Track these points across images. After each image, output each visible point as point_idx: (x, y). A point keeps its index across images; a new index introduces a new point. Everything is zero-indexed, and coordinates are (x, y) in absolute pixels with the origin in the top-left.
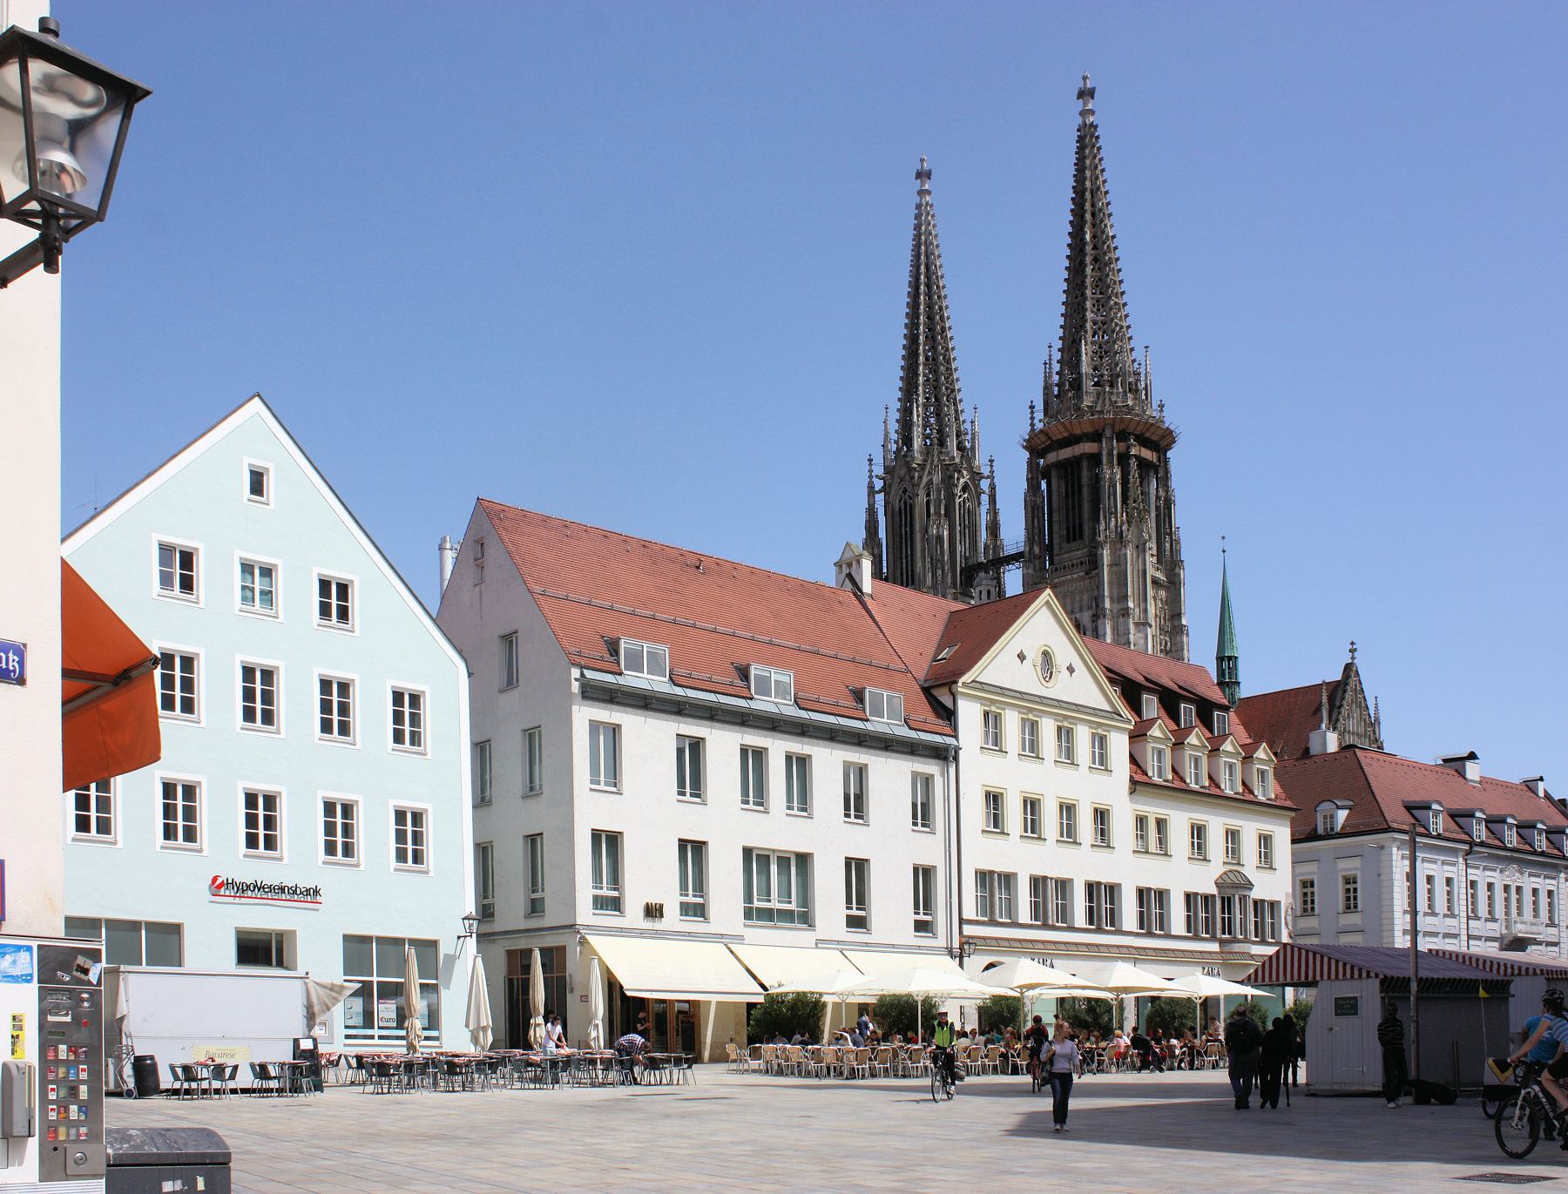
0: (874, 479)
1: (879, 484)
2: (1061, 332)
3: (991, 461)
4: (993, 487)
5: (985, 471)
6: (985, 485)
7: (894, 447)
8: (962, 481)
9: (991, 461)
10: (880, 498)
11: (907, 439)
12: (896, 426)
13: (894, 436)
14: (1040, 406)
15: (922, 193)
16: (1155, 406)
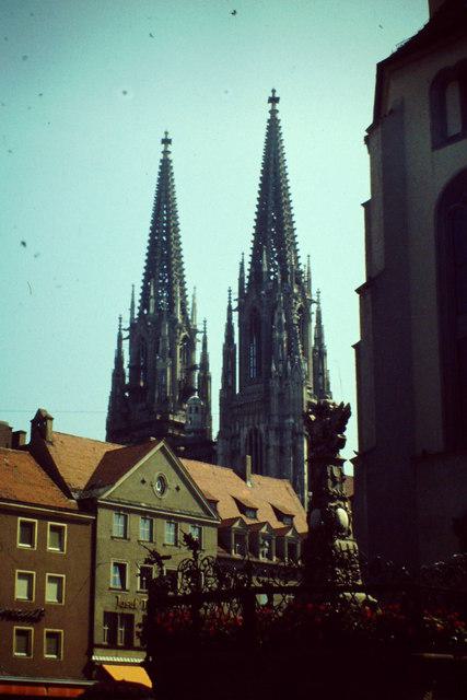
0: (123, 332)
1: (126, 334)
2: (252, 245)
3: (205, 322)
4: (205, 338)
5: (200, 328)
6: (199, 336)
7: (137, 311)
8: (183, 334)
9: (205, 322)
10: (126, 344)
11: (145, 303)
12: (140, 297)
13: (138, 304)
14: (235, 290)
15: (166, 152)
16: (314, 291)
